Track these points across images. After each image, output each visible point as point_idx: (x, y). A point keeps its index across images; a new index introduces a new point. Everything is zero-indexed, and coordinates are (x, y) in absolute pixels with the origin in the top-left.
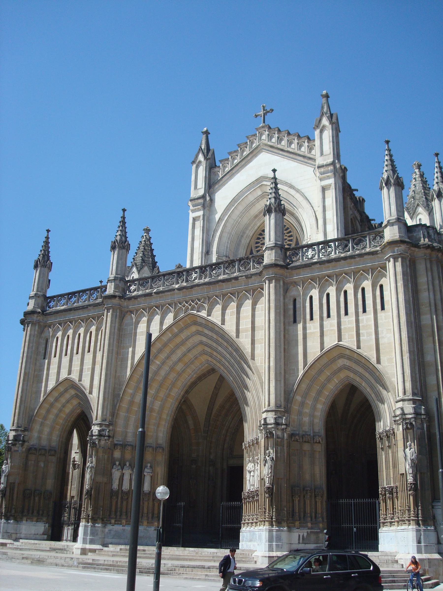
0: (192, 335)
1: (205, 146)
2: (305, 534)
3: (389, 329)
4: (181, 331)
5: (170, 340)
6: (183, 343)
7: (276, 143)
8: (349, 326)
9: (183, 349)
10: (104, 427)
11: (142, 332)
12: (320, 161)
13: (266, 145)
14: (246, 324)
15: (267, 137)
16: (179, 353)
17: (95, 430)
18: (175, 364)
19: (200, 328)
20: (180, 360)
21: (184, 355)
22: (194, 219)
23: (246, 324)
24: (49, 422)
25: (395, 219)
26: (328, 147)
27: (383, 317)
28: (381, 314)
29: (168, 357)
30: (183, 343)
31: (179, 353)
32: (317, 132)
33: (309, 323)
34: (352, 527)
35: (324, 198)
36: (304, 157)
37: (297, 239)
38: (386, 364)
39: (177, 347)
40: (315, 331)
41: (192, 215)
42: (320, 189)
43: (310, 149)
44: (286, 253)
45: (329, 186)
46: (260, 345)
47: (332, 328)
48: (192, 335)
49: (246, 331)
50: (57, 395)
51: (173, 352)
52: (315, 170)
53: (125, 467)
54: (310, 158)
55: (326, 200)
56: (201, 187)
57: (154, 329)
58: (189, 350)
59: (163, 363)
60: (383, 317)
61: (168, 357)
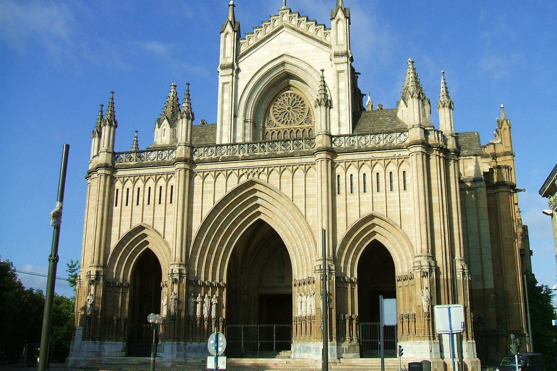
1: (232, 18)
2: (347, 347)
3: (410, 205)
7: (297, 26)
8: (380, 200)
10: (182, 267)
11: (209, 191)
12: (335, 49)
13: (288, 27)
14: (299, 192)
15: (288, 20)
22: (224, 84)
23: (299, 192)
25: (418, 125)
26: (342, 38)
28: (403, 193)
32: (333, 22)
34: (378, 341)
35: (338, 81)
36: (321, 42)
37: (309, 110)
40: (355, 201)
41: (221, 80)
42: (336, 73)
43: (326, 35)
44: (331, 139)
45: (342, 71)
46: (311, 209)
47: (368, 201)
49: (300, 197)
52: (331, 56)
54: (327, 45)
55: (340, 83)
56: (229, 56)
57: (220, 189)
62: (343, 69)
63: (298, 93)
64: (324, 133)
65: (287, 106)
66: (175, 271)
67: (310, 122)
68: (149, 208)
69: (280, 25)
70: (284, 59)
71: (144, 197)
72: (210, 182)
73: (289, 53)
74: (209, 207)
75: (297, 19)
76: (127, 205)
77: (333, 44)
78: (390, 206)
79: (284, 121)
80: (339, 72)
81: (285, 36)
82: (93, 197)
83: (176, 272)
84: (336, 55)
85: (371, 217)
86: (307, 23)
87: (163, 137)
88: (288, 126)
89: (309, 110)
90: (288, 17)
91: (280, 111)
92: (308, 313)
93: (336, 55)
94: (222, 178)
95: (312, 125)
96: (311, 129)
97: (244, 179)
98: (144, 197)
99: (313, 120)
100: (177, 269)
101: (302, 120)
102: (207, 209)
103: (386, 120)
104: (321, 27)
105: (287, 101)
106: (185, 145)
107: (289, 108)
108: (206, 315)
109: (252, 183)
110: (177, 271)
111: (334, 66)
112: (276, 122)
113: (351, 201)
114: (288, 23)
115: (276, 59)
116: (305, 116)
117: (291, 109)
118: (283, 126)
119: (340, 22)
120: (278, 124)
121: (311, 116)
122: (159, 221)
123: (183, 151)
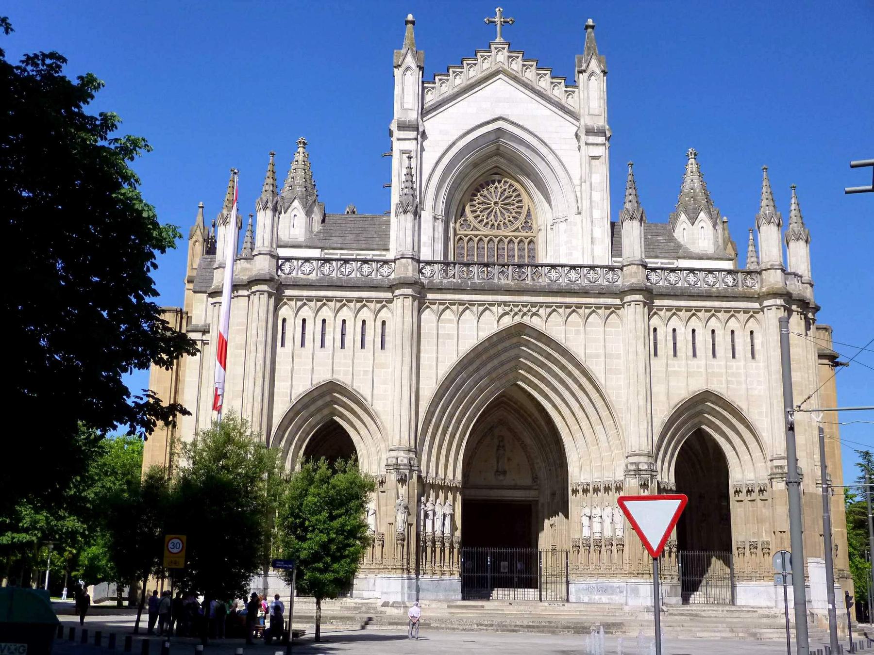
8: (718, 370)
9: (496, 362)
12: (586, 121)
16: (489, 367)
17: (402, 458)
21: (495, 369)
27: (754, 367)
30: (498, 355)
31: (489, 367)
33: (673, 360)
37: (529, 209)
38: (757, 417)
39: (491, 359)
46: (614, 376)
47: (699, 370)
50: (308, 400)
51: (484, 364)
58: (502, 364)
60: (754, 367)
62: (600, 154)
64: (639, 263)
65: (496, 197)
66: (402, 461)
67: (531, 228)
68: (344, 355)
69: (494, 68)
70: (500, 124)
71: (333, 334)
72: (450, 321)
73: (508, 115)
74: (449, 359)
75: (521, 62)
76: (303, 345)
78: (731, 381)
79: (487, 223)
81: (500, 87)
82: (238, 328)
83: (403, 463)
84: (589, 132)
85: (706, 396)
86: (537, 72)
87: (292, 228)
88: (495, 232)
89: (529, 209)
90: (506, 57)
91: (482, 207)
93: (589, 132)
95: (534, 234)
97: (507, 321)
98: (333, 334)
99: (534, 226)
100: (404, 457)
101: (518, 224)
102: (445, 363)
103: (658, 241)
104: (560, 81)
105: (500, 190)
106: (412, 258)
107: (496, 203)
108: (438, 533)
109: (520, 329)
110: (405, 461)
111: (583, 147)
112: (474, 223)
113: (674, 369)
114: (506, 67)
115: (488, 123)
117: (499, 207)
118: (486, 231)
119: (593, 78)
120: (477, 225)
122: (361, 377)
123: (410, 268)
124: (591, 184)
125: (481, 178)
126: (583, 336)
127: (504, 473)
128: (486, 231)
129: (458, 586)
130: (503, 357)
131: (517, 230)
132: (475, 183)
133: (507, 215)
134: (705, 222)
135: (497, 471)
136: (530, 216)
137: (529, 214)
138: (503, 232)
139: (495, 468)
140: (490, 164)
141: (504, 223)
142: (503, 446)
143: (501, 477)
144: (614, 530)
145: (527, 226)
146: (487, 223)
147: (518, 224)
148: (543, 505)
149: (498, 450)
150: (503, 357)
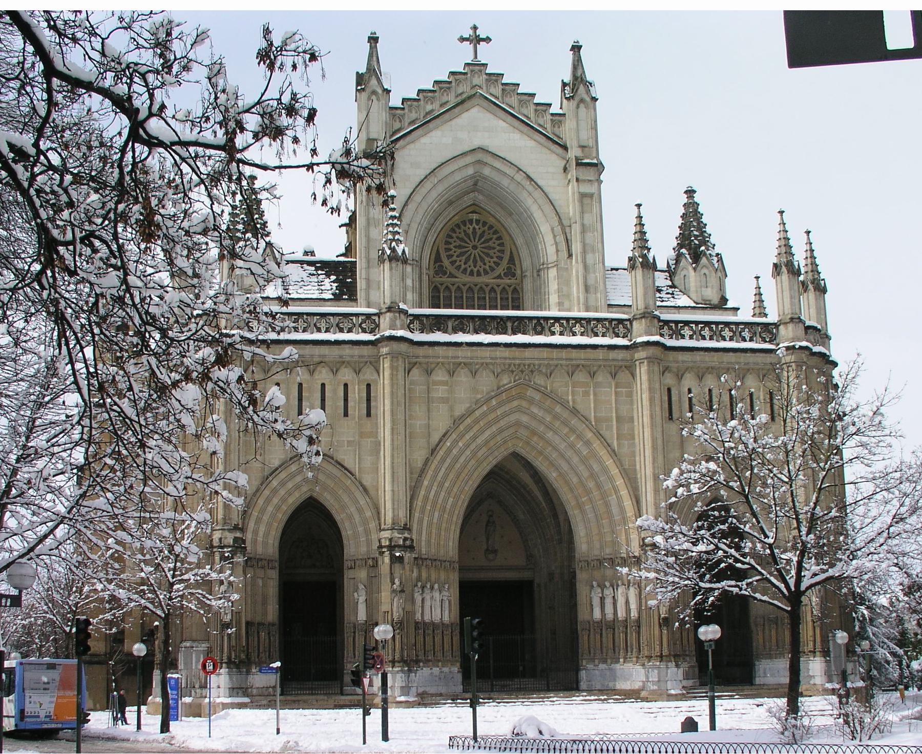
0: (511, 412)
4: (500, 404)
5: (484, 415)
6: (497, 420)
9: (494, 428)
16: (487, 433)
18: (480, 448)
19: (524, 404)
20: (487, 442)
21: (493, 436)
24: (265, 518)
29: (474, 438)
30: (497, 420)
31: (487, 433)
35: (582, 212)
39: (489, 425)
48: (511, 412)
51: (482, 431)
53: (425, 590)
58: (501, 431)
59: (467, 446)
61: (474, 438)
63: (491, 220)
67: (514, 275)
70: (480, 156)
72: (444, 383)
77: (571, 143)
80: (583, 196)
92: (619, 615)
94: (463, 377)
96: (515, 289)
99: (518, 272)
101: (500, 270)
107: (475, 247)
112: (451, 269)
115: (464, 154)
116: (504, 263)
119: (582, 105)
120: (454, 272)
121: (514, 265)
124: (583, 225)
125: (456, 218)
126: (592, 397)
127: (495, 552)
128: (466, 279)
129: (459, 677)
130: (502, 423)
131: (499, 277)
132: (451, 222)
133: (487, 259)
134: (707, 268)
135: (487, 550)
136: (513, 260)
137: (512, 260)
138: (484, 279)
139: (485, 547)
140: (467, 200)
141: (484, 270)
142: (494, 522)
143: (491, 556)
144: (628, 610)
145: (510, 273)
146: (465, 269)
147: (500, 270)
148: (539, 585)
149: (487, 525)
150: (502, 423)
